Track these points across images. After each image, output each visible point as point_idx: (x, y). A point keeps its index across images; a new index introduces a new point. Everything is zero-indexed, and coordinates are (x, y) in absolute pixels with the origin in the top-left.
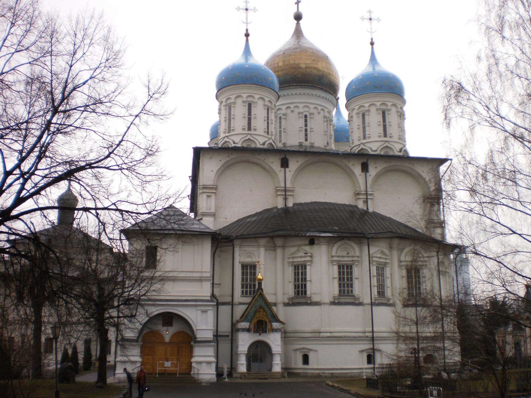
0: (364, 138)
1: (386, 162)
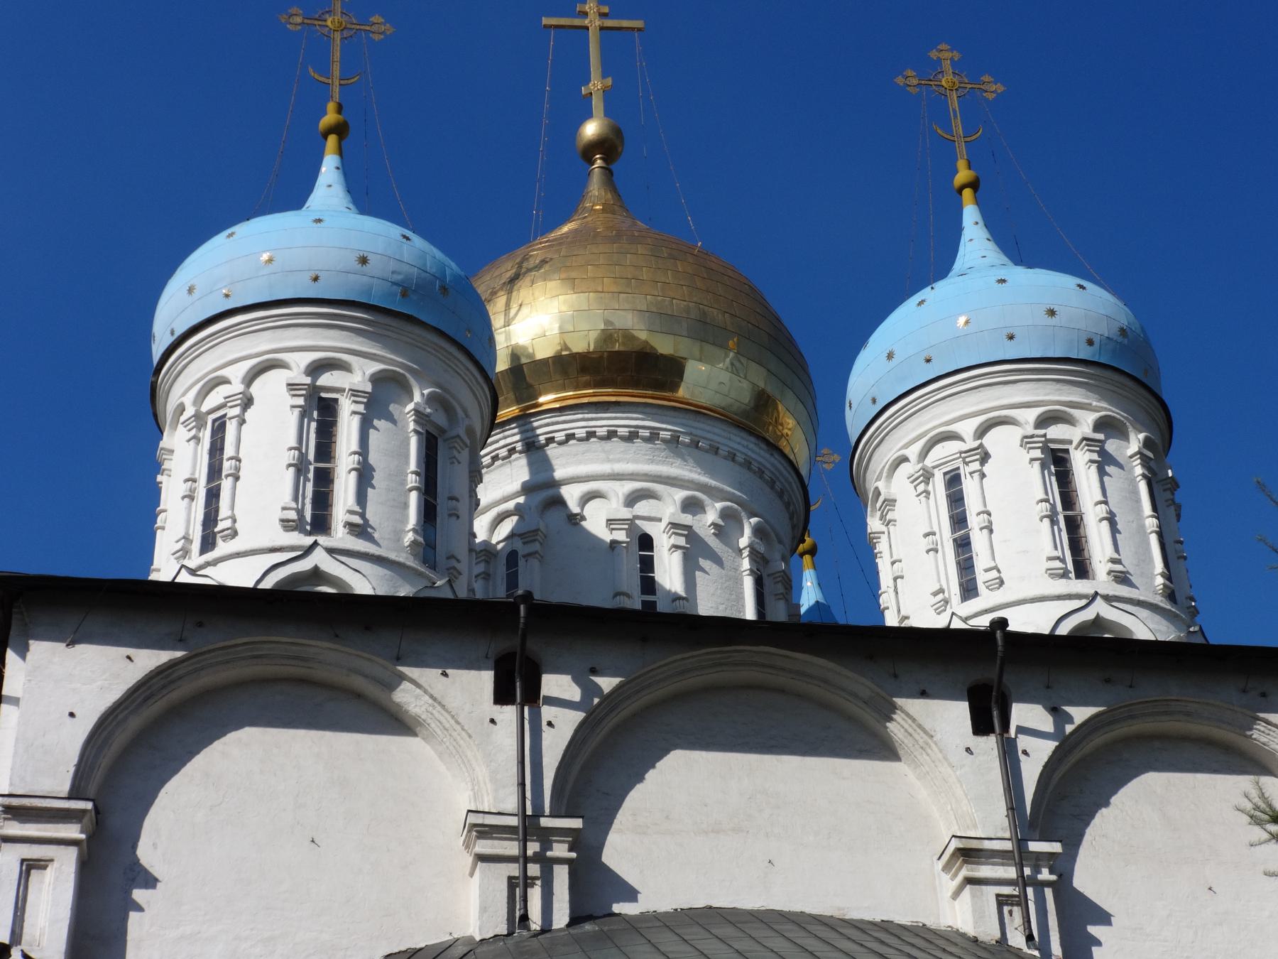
1: (1108, 681)
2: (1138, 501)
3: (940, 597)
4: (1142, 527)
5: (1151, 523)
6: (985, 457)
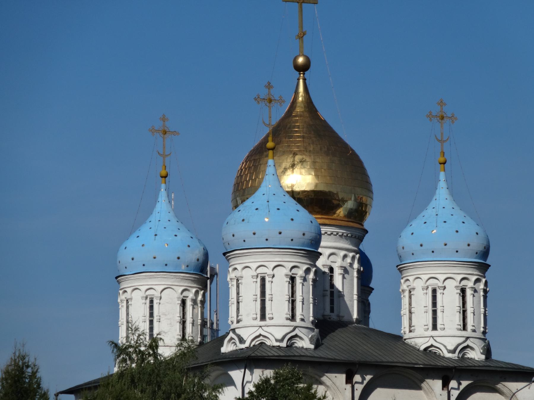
0: (435, 327)
2: (480, 303)
3: (426, 327)
4: (480, 312)
5: (482, 310)
6: (445, 288)
